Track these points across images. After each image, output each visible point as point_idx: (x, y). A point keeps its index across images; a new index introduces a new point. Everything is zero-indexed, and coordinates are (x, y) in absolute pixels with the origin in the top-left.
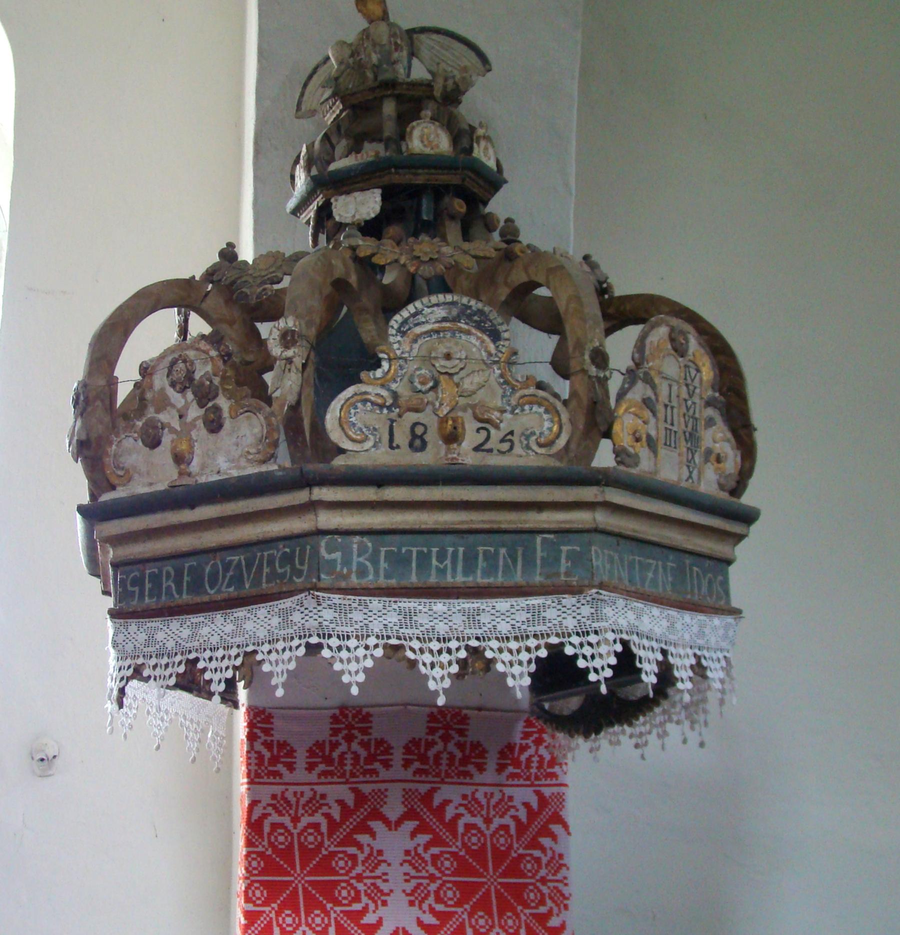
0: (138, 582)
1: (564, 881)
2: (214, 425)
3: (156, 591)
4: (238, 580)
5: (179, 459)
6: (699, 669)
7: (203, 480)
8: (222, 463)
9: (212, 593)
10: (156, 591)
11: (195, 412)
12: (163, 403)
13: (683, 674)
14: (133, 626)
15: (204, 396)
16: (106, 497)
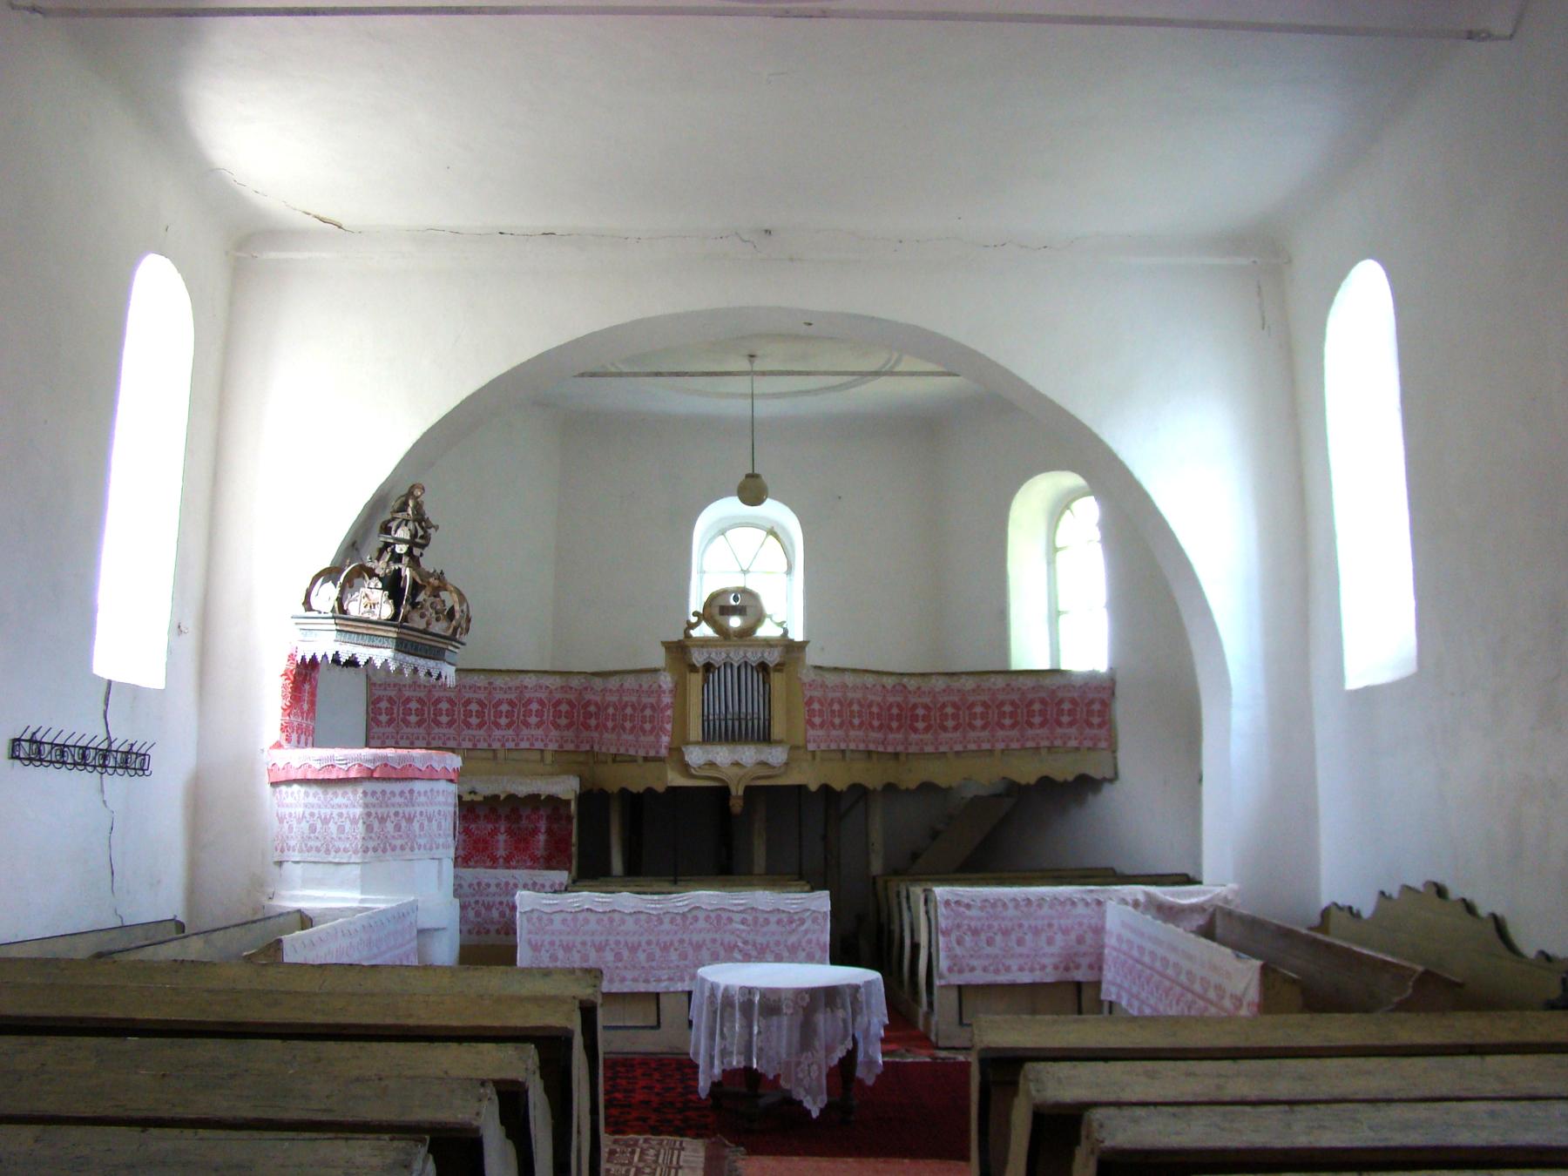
0: (402, 643)
1: (283, 692)
2: (438, 620)
3: (406, 647)
4: (426, 652)
5: (428, 624)
6: (446, 678)
7: (434, 631)
8: (437, 628)
9: (419, 653)
10: (406, 647)
11: (434, 615)
12: (427, 610)
13: (444, 677)
14: (400, 654)
15: (437, 613)
16: (405, 624)
